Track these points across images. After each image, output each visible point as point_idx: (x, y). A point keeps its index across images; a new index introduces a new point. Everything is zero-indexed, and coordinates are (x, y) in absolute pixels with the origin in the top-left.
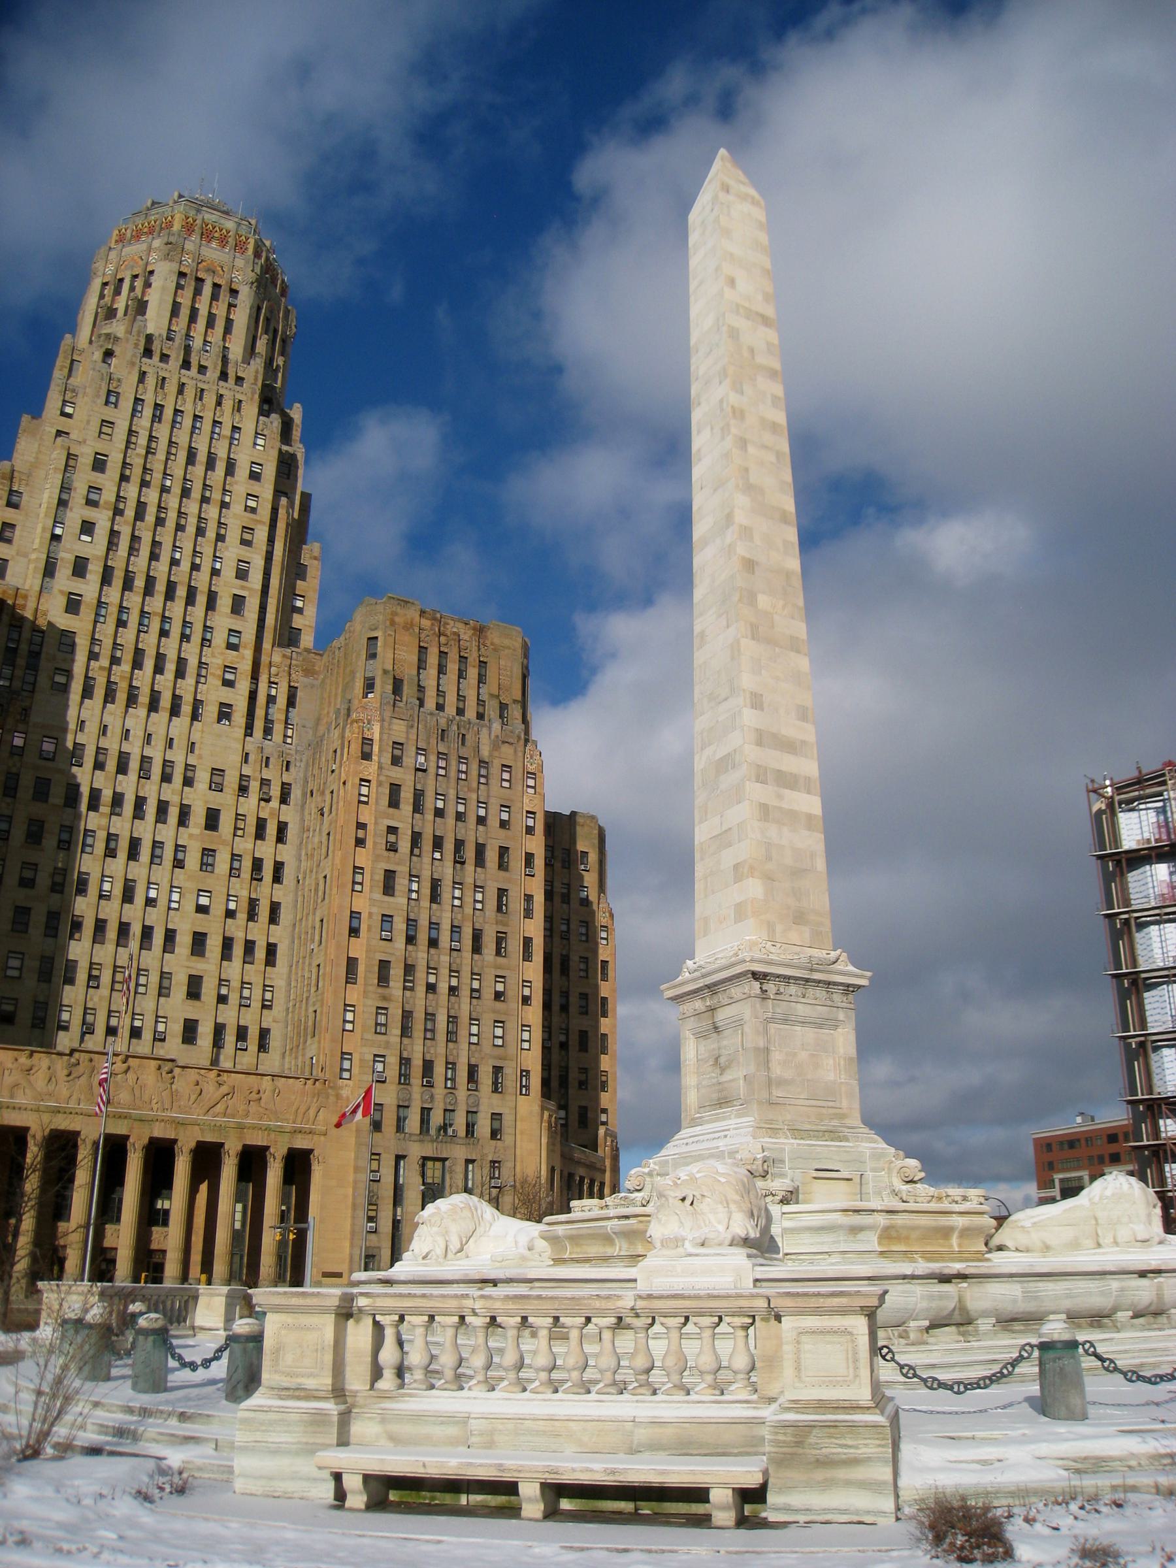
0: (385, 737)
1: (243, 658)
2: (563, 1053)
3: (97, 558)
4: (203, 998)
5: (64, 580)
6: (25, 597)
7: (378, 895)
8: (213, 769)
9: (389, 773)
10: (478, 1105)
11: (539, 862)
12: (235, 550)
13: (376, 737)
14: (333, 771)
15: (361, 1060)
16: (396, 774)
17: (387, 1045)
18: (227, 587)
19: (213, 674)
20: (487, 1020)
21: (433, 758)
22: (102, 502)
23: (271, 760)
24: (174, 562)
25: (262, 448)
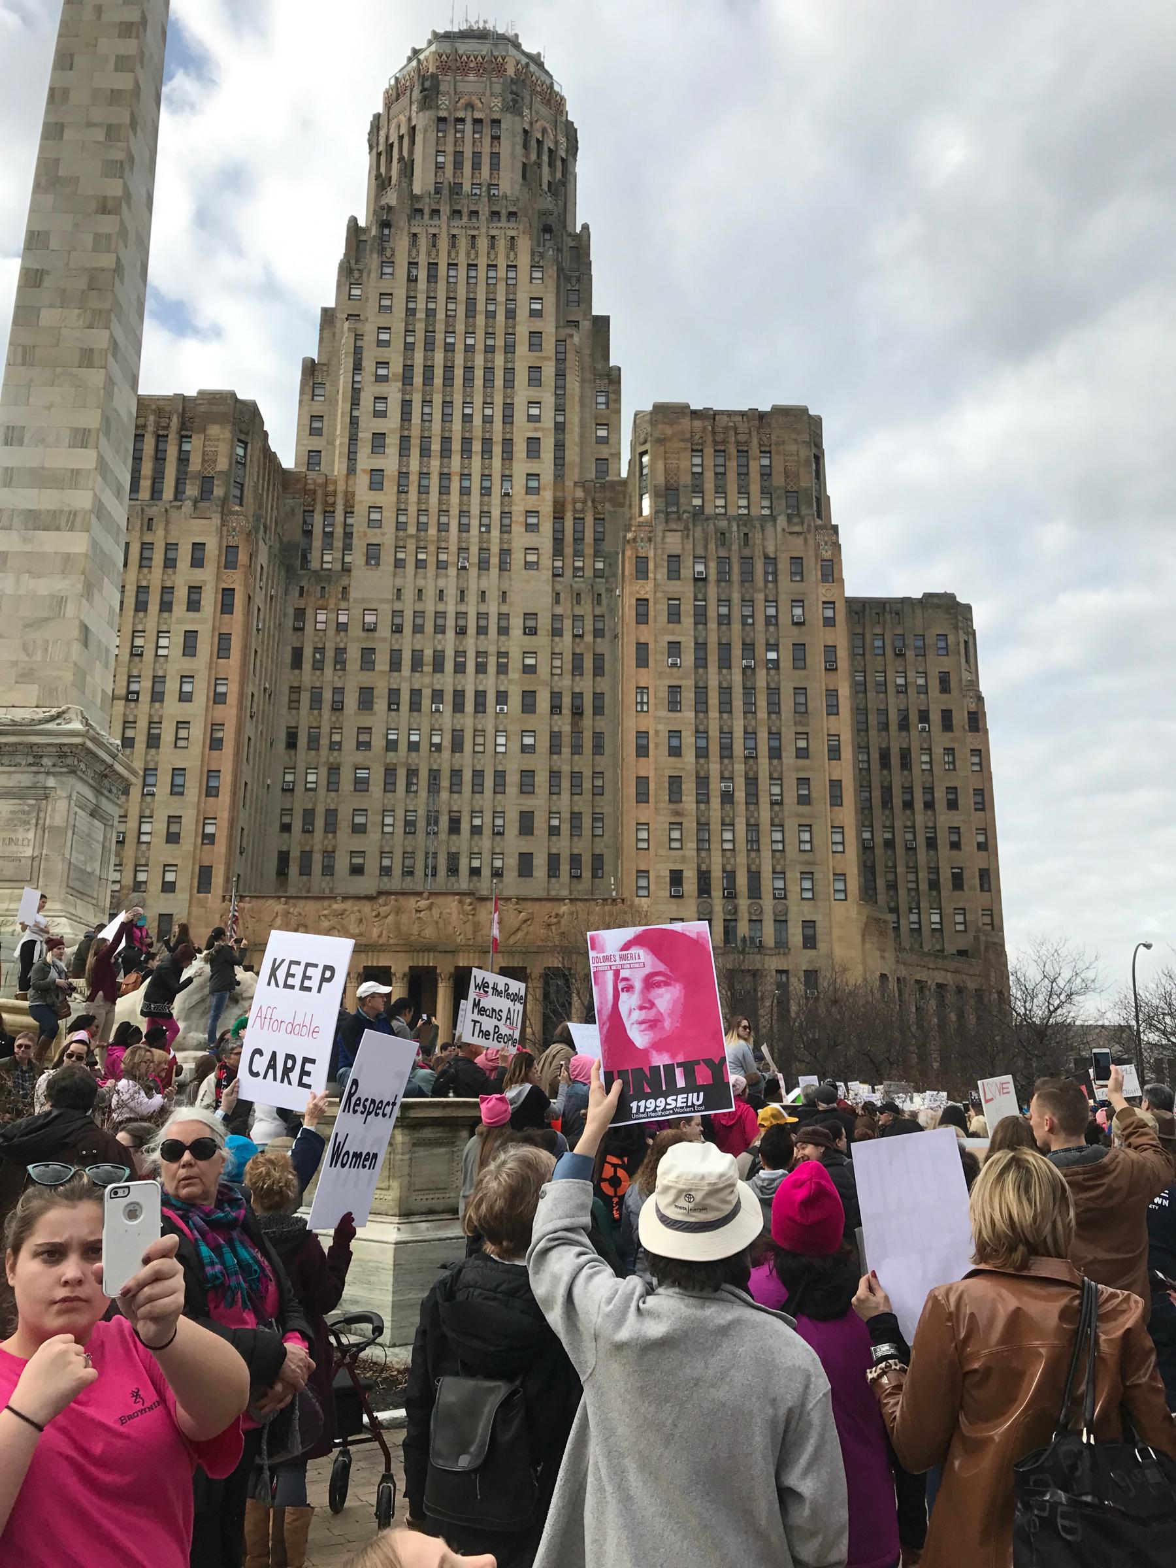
0: (659, 551)
1: (544, 500)
2: (932, 852)
4: (535, 832)
5: (365, 461)
6: (335, 482)
7: (663, 713)
9: (666, 589)
10: (786, 914)
11: (842, 654)
13: (651, 554)
15: (657, 877)
16: (674, 587)
17: (683, 859)
18: (522, 431)
20: (791, 825)
21: (713, 565)
23: (583, 596)
24: (467, 419)
25: (539, 281)
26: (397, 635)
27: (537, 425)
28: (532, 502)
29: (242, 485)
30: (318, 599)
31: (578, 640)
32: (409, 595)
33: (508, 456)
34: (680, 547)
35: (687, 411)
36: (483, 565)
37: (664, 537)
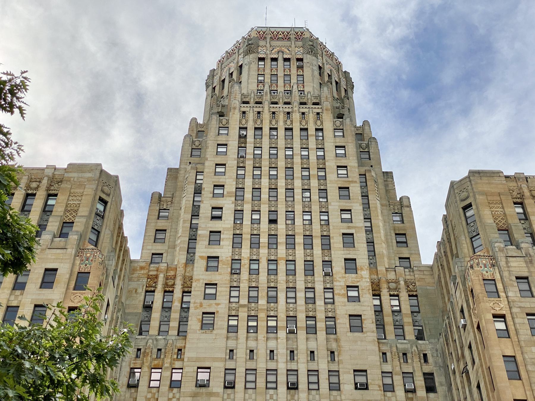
1: (362, 277)
3: (227, 229)
8: (355, 371)
9: (522, 305)
12: (337, 204)
13: (497, 277)
14: (464, 326)
19: (339, 294)
22: (225, 193)
23: (409, 355)
26: (229, 391)
27: (350, 225)
28: (351, 279)
29: (99, 232)
30: (155, 359)
31: (410, 395)
32: (241, 354)
33: (327, 246)
34: (527, 270)
35: (501, 175)
36: (312, 330)
37: (507, 262)
